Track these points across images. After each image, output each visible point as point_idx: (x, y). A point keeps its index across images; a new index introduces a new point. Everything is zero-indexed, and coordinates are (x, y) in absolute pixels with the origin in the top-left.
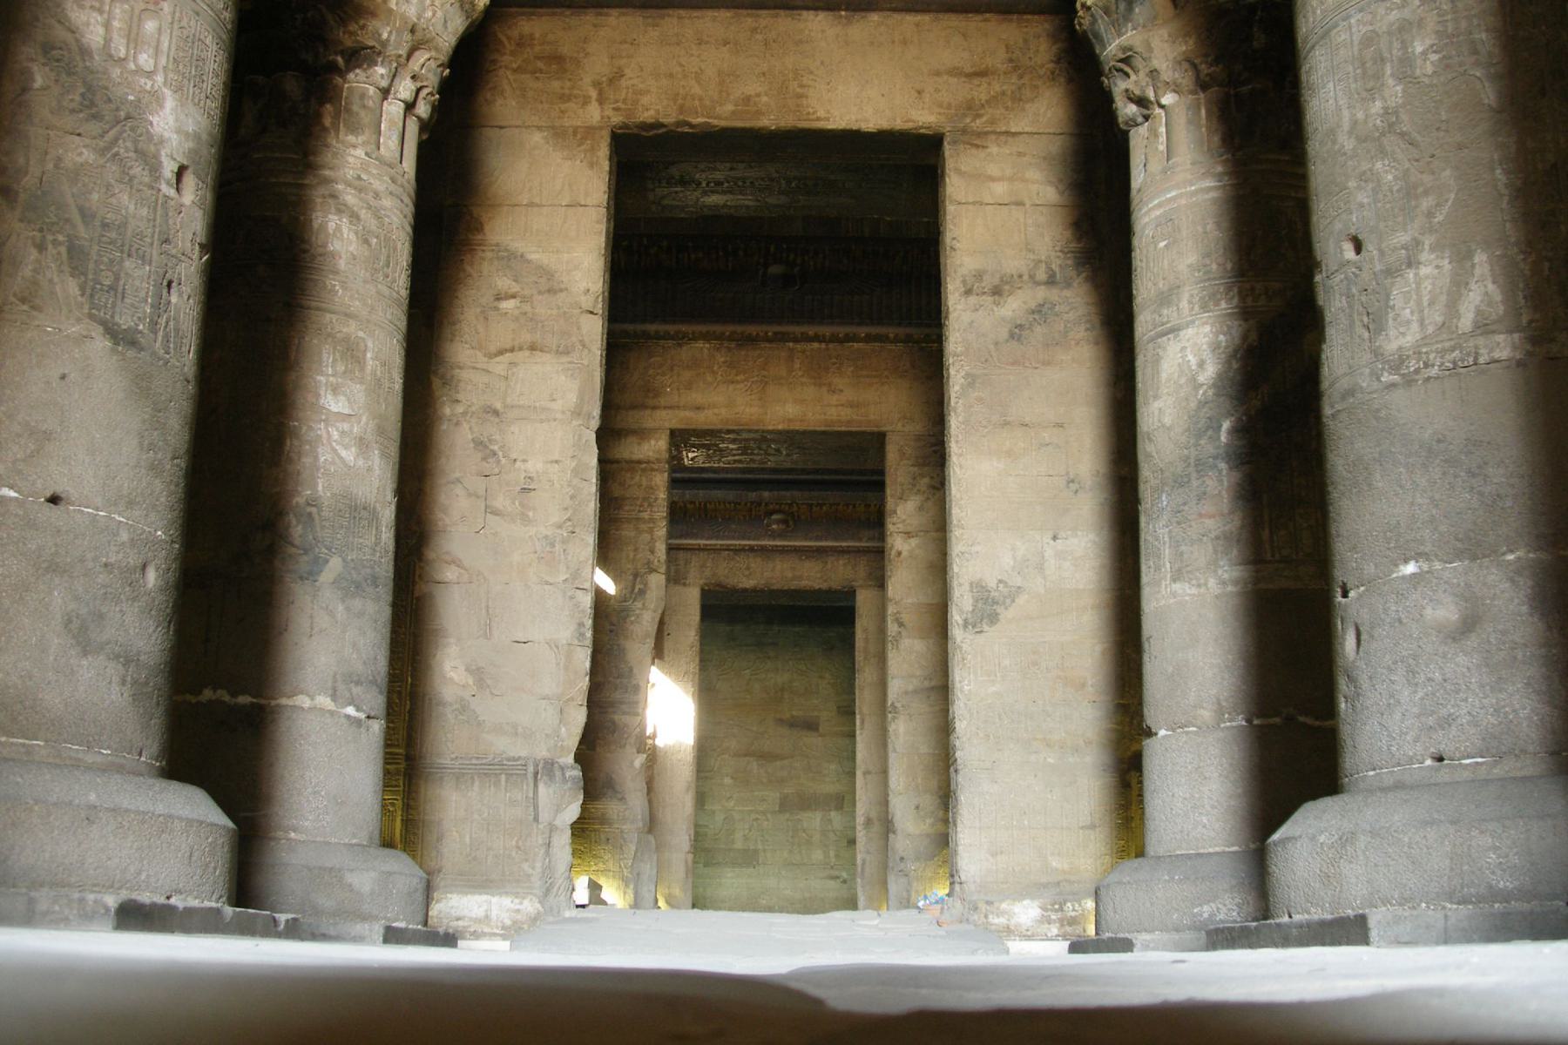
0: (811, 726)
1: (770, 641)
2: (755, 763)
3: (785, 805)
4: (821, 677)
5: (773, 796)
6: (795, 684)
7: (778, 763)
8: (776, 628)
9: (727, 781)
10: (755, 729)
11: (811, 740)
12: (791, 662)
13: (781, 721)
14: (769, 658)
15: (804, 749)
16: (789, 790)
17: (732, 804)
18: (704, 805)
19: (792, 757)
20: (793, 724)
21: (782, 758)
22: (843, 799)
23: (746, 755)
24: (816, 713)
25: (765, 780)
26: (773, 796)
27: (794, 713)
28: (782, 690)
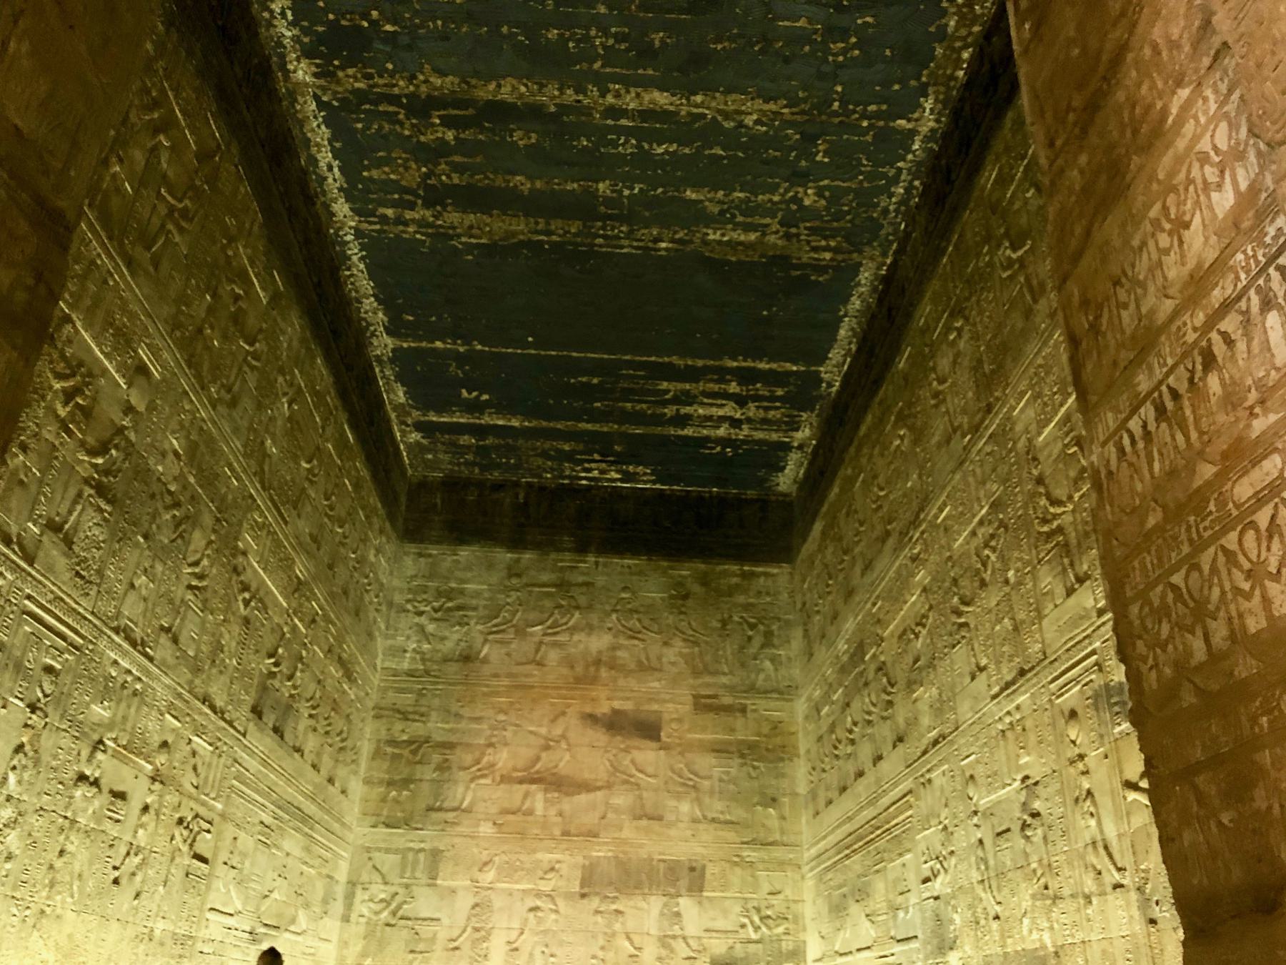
0: (648, 729)
1: (581, 579)
2: (540, 796)
3: (590, 883)
4: (666, 644)
5: (569, 862)
6: (619, 653)
7: (583, 798)
8: (591, 558)
9: (486, 829)
10: (543, 731)
11: (647, 755)
12: (614, 616)
13: (592, 719)
14: (578, 608)
15: (634, 772)
16: (600, 852)
17: (489, 876)
18: (434, 878)
19: (609, 786)
20: (616, 724)
21: (587, 787)
22: (704, 867)
23: (521, 781)
24: (655, 707)
25: (557, 832)
26: (569, 862)
27: (617, 704)
28: (598, 662)
